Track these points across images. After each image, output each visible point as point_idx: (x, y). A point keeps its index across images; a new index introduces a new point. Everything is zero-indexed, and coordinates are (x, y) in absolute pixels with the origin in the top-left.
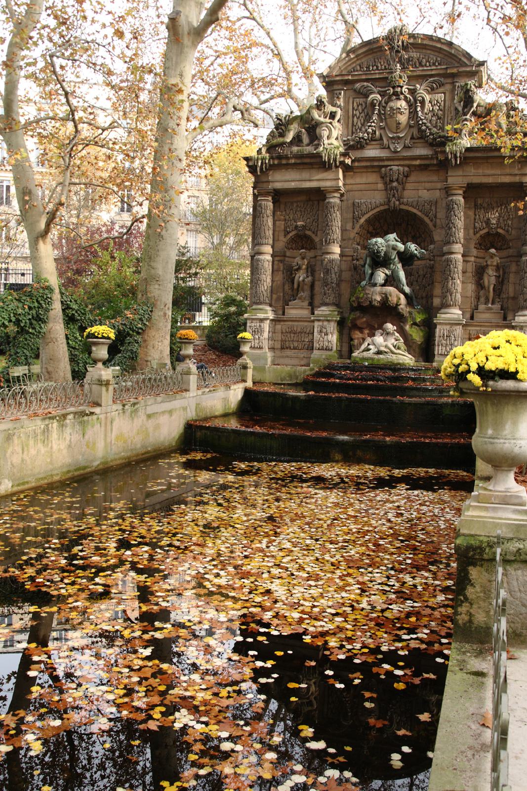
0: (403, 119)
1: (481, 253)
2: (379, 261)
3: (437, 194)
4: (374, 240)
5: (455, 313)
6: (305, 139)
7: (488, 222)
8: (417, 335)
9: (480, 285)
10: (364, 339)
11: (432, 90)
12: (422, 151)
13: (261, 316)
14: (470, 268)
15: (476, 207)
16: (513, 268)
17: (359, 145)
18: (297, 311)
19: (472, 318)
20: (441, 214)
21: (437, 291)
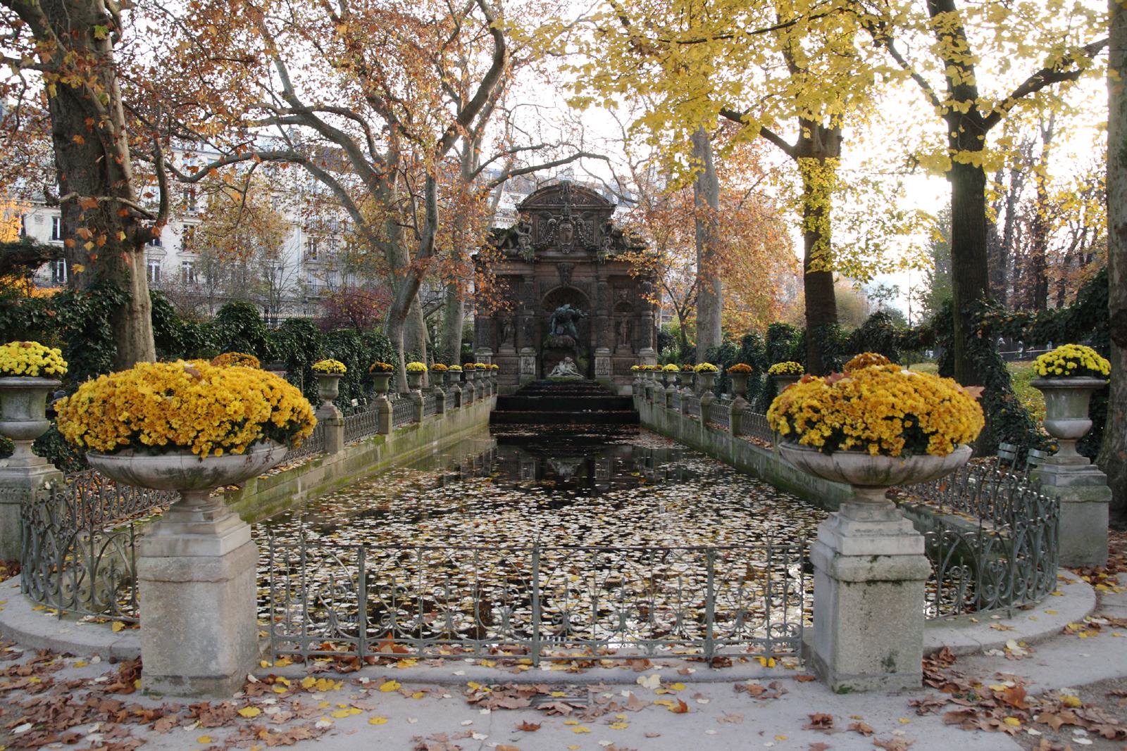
0: (570, 234)
1: (617, 314)
2: (561, 320)
3: (591, 279)
4: (559, 309)
5: (606, 350)
6: (511, 245)
7: (621, 296)
8: (584, 363)
9: (618, 333)
10: (553, 368)
11: (586, 218)
12: (582, 254)
13: (487, 354)
14: (612, 323)
15: (615, 288)
16: (637, 323)
17: (544, 248)
18: (507, 350)
19: (614, 352)
20: (594, 291)
21: (594, 337)
